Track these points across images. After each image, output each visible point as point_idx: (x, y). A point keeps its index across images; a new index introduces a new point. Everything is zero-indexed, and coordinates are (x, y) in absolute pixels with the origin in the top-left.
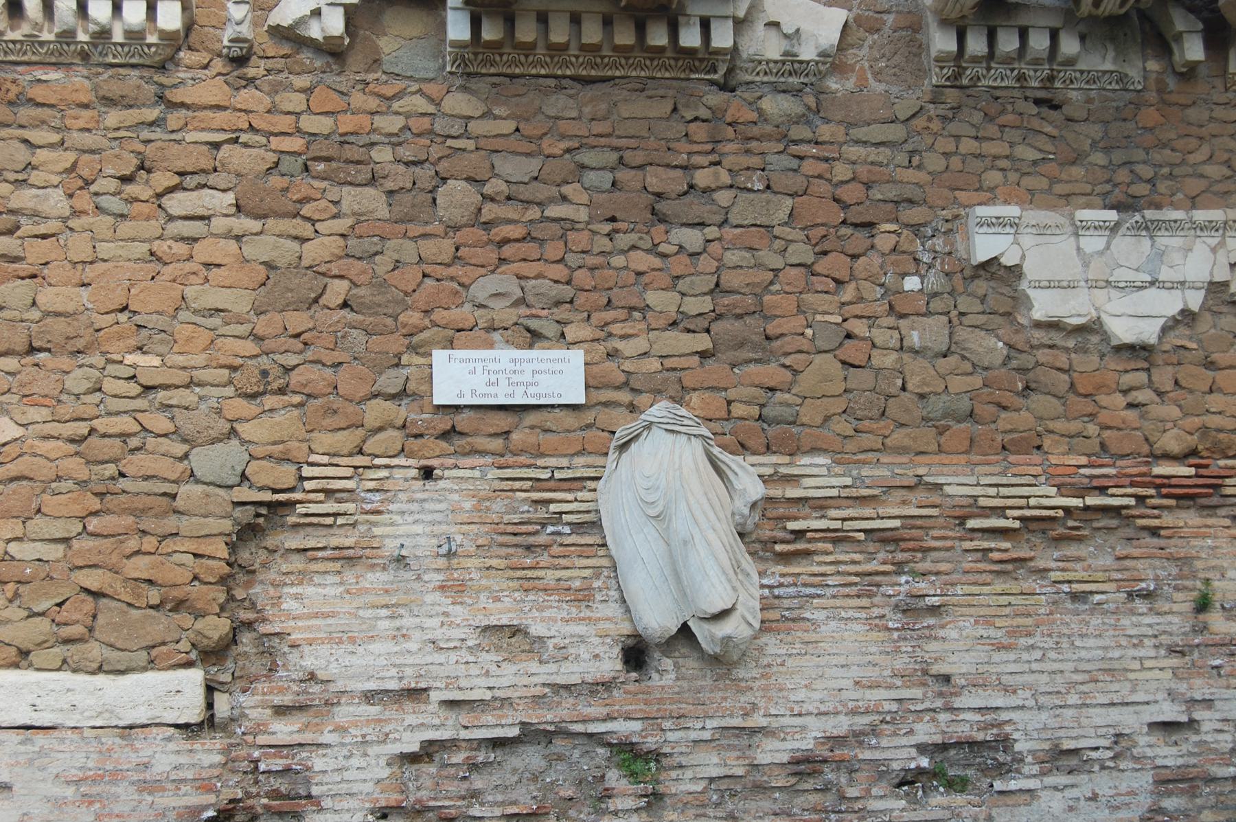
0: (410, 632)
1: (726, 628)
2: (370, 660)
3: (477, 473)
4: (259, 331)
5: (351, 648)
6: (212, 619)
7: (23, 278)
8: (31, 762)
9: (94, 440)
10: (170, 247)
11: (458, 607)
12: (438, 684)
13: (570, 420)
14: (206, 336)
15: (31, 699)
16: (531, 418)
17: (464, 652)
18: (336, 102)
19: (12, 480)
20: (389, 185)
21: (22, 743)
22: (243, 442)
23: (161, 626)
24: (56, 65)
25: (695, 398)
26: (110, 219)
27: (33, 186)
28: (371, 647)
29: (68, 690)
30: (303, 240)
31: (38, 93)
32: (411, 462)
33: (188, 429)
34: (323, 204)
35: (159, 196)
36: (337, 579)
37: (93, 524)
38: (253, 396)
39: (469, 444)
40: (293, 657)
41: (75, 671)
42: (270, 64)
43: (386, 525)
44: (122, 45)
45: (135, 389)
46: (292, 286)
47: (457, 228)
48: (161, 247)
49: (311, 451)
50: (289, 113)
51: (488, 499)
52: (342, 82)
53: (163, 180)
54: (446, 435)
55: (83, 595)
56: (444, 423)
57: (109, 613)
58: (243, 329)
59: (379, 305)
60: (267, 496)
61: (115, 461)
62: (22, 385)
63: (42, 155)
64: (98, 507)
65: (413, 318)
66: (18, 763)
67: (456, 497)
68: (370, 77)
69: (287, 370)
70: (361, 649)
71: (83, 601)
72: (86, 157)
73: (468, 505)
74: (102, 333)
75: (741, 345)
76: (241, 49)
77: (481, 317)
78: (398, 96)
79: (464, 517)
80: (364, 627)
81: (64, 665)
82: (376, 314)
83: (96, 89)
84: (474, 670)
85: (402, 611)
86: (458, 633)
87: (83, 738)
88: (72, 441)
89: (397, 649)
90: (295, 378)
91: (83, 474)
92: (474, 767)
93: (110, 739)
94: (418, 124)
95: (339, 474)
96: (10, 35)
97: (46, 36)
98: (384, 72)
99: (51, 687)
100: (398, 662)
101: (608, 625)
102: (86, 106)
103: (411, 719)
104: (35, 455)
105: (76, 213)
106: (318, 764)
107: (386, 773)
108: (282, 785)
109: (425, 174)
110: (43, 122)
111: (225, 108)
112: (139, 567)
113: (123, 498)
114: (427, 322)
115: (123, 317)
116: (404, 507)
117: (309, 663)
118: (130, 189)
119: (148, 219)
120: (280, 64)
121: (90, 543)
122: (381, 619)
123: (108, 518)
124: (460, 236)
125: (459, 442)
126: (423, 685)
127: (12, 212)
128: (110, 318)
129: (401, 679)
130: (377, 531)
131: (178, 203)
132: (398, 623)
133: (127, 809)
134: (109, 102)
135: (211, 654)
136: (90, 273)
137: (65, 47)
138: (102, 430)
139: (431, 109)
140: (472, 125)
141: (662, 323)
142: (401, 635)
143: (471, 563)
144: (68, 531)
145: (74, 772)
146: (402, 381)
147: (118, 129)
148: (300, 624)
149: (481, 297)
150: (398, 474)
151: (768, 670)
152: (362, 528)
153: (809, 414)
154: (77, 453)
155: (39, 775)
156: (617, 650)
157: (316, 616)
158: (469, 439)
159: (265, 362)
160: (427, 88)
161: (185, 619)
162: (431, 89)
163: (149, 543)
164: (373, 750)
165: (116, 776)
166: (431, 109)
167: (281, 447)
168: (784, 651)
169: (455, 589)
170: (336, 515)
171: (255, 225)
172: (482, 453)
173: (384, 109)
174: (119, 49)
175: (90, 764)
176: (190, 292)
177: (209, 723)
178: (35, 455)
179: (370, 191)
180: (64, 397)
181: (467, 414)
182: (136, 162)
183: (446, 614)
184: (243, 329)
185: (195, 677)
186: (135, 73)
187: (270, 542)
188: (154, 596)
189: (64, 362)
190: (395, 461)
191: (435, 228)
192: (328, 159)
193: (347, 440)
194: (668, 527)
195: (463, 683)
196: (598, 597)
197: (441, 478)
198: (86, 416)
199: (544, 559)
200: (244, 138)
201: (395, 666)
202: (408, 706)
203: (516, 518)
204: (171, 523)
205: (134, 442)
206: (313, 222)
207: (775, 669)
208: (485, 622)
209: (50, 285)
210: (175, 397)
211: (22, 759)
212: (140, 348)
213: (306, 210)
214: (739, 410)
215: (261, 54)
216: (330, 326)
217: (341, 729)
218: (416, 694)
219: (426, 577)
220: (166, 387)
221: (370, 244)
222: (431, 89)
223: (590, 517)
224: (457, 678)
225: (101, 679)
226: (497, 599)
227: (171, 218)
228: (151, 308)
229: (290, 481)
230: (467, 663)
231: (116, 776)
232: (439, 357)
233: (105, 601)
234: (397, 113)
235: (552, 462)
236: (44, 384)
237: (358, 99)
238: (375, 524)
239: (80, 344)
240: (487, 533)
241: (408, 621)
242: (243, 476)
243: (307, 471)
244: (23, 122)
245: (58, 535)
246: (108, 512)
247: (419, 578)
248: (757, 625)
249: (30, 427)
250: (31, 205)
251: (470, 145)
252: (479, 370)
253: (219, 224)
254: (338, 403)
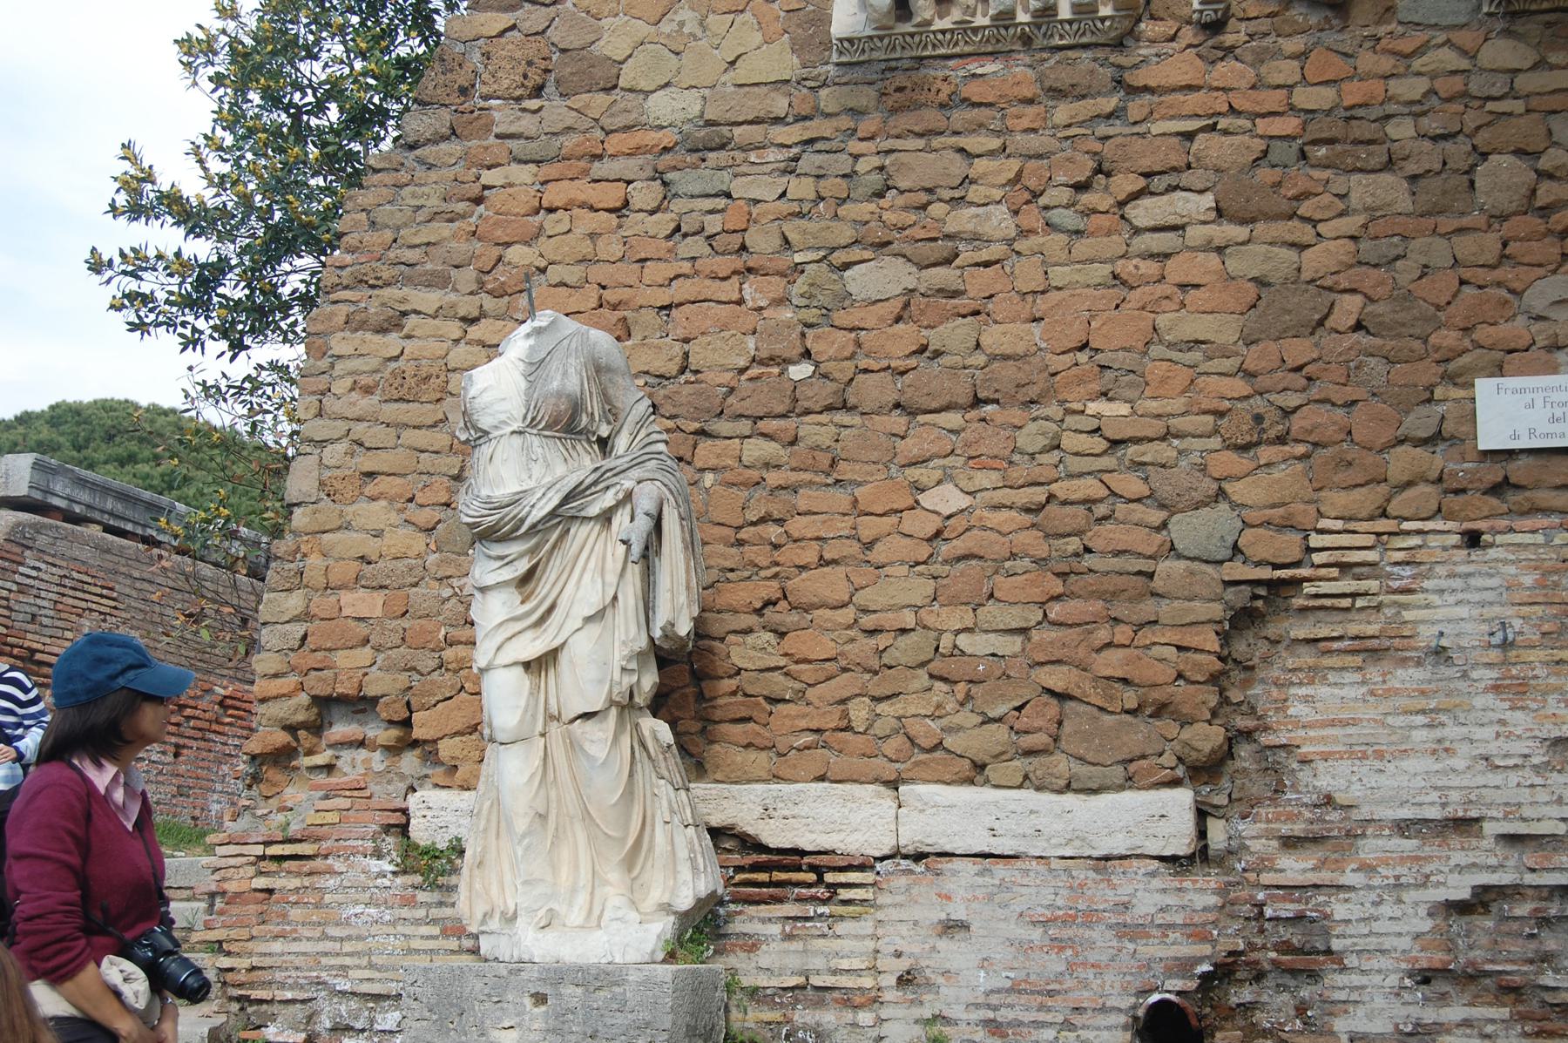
0: (1455, 745)
2: (1403, 781)
3: (1540, 538)
4: (1250, 365)
5: (1378, 764)
6: (1201, 727)
7: (964, 316)
8: (990, 897)
9: (1052, 508)
10: (1136, 267)
11: (1519, 714)
12: (1494, 813)
14: (1183, 375)
15: (989, 821)
17: (1527, 772)
18: (1339, 67)
19: (959, 559)
20: (1412, 168)
21: (980, 874)
22: (1234, 506)
23: (1139, 735)
24: (993, 54)
26: (1064, 238)
27: (971, 204)
28: (1404, 764)
29: (1032, 812)
30: (1302, 247)
31: (974, 91)
32: (1450, 525)
33: (1165, 491)
34: (1326, 199)
35: (1121, 204)
36: (1357, 677)
37: (1055, 611)
38: (1245, 448)
39: (1527, 499)
40: (1304, 775)
41: (1038, 789)
42: (1252, 26)
43: (1419, 607)
44: (1070, 22)
45: (1099, 444)
46: (1290, 307)
47: (1503, 218)
48: (1126, 268)
49: (1321, 515)
50: (1278, 87)
51: (1556, 571)
52: (1346, 41)
53: (1125, 183)
54: (1496, 489)
55: (1046, 698)
56: (1494, 474)
57: (1077, 718)
58: (1229, 364)
59: (1404, 325)
60: (1266, 573)
61: (1079, 533)
62: (968, 445)
63: (981, 165)
64: (1060, 590)
65: (1448, 338)
66: (975, 898)
67: (1512, 570)
68: (1382, 30)
69: (1287, 413)
70: (1391, 767)
71: (1046, 704)
72: (1033, 163)
73: (1528, 580)
74: (1058, 378)
76: (1216, 11)
77: (1540, 332)
78: (1419, 51)
79: (1525, 596)
80: (1394, 738)
81: (1025, 781)
82: (1399, 336)
83: (1040, 79)
84: (1543, 796)
85: (1443, 718)
86: (1520, 747)
87: (1051, 870)
88: (1028, 510)
89: (1438, 766)
90: (1297, 423)
91: (1042, 552)
92: (1544, 922)
93: (1082, 873)
94: (1446, 86)
95: (1358, 544)
96: (939, 24)
97: (981, 21)
98: (1400, 23)
99: (1012, 807)
100: (1440, 783)
102: (1030, 101)
103: (1459, 858)
104: (984, 528)
105: (1024, 233)
106: (1339, 911)
107: (1426, 925)
108: (1294, 936)
109: (1458, 151)
110: (981, 125)
111: (1198, 88)
112: (1111, 663)
113: (1090, 578)
114: (1467, 343)
115: (1082, 357)
116: (1444, 584)
117: (1324, 783)
118: (1086, 199)
119: (1109, 234)
120: (1264, 25)
121: (1053, 634)
122: (1416, 728)
123: (1072, 603)
124: (1507, 229)
125: (1514, 498)
126: (1474, 814)
127: (948, 237)
128: (1068, 358)
129: (1444, 805)
130: (1408, 615)
131: (1142, 213)
132: (1438, 733)
133: (1104, 958)
134: (1057, 93)
135: (1202, 771)
136: (1042, 304)
137: (1003, 32)
138: (1062, 495)
139: (1464, 64)
140: (1520, 81)
142: (1442, 749)
143: (1534, 656)
144: (1026, 620)
145: (1040, 910)
146: (1436, 421)
147: (1069, 126)
148: (1312, 733)
149: (1539, 306)
150: (1434, 541)
152: (1389, 612)
154: (1033, 525)
155: (1000, 913)
157: (1332, 723)
158: (1528, 494)
159: (1258, 404)
160: (1456, 37)
161: (1168, 726)
162: (1465, 38)
163: (1123, 634)
164: (1409, 896)
165: (1090, 917)
166: (1464, 64)
167: (1281, 510)
169: (1515, 690)
170: (1354, 595)
171: (1241, 232)
172: (1546, 511)
173: (1402, 70)
174: (1067, 27)
175: (1060, 902)
176: (1162, 321)
177: (1201, 856)
178: (984, 528)
179: (1386, 178)
180: (1016, 458)
181: (1523, 461)
182: (1091, 164)
183: (1502, 722)
184: (1229, 364)
185: (1181, 799)
186: (1086, 55)
187: (1271, 630)
188: (1130, 698)
189: (1016, 415)
190: (1430, 525)
191: (1475, 218)
192: (1330, 141)
193: (1365, 499)
195: (1527, 812)
197: (1492, 545)
198: (1042, 480)
200: (1223, 123)
201: (1435, 788)
202: (1455, 841)
204: (1148, 608)
205: (1101, 510)
206: (1314, 222)
208: (1556, 733)
209: (996, 322)
210: (1149, 453)
211: (979, 893)
212: (1105, 394)
213: (1305, 209)
215: (1241, 15)
216: (1340, 354)
217: (1367, 868)
218: (1464, 825)
219: (1475, 675)
220: (1137, 441)
221: (1389, 247)
222: (1465, 38)
224: (1519, 805)
225: (1069, 799)
227: (1137, 231)
228: (1116, 344)
229: (1295, 554)
230: (1532, 786)
231: (1090, 917)
232: (1485, 388)
233: (1072, 704)
234: (1419, 74)
236: (993, 443)
237: (1367, 61)
238: (1406, 606)
239: (1033, 392)
240: (1555, 616)
241: (1452, 731)
242: (1236, 549)
243: (1316, 541)
244: (958, 127)
245: (1014, 625)
246: (1072, 595)
247: (1465, 676)
249: (978, 495)
250: (970, 227)
251: (1518, 106)
252: (1539, 403)
253: (1196, 234)
254: (1353, 453)
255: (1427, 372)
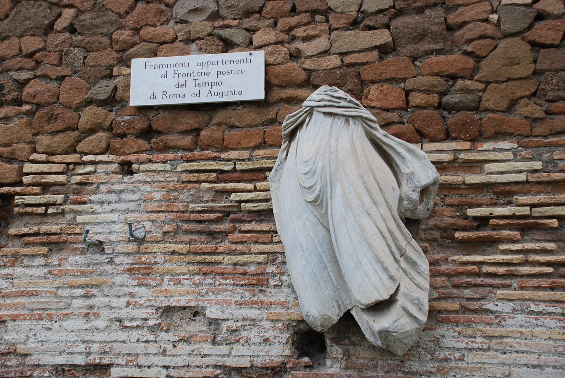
0: (100, 311)
1: (384, 322)
2: (63, 335)
3: (168, 167)
5: (48, 324)
11: (143, 289)
12: (119, 361)
13: (251, 116)
16: (219, 116)
17: (145, 332)
25: (373, 91)
28: (65, 324)
32: (112, 157)
36: (42, 261)
39: (161, 141)
43: (87, 213)
46: (29, 15)
49: (35, 151)
51: (176, 190)
56: (141, 124)
59: (97, 27)
65: (124, 35)
67: (147, 188)
69: (22, 84)
70: (56, 325)
73: (158, 195)
75: (421, 37)
77: (180, 30)
79: (153, 206)
80: (61, 305)
82: (94, 34)
84: (152, 348)
85: (95, 291)
86: (141, 313)
89: (87, 326)
90: (27, 90)
100: (86, 338)
101: (280, 310)
114: (136, 39)
116: (103, 197)
122: (76, 298)
126: (106, 361)
129: (88, 354)
130: (80, 219)
132: (90, 302)
141: (342, 22)
142: (89, 314)
143: (156, 248)
146: (110, 89)
148: (8, 301)
150: (101, 168)
151: (444, 364)
152: (69, 217)
153: (490, 99)
156: (286, 335)
157: (22, 294)
158: (163, 137)
167: (9, 149)
168: (463, 345)
169: (141, 271)
170: (47, 205)
172: (175, 148)
183: (132, 295)
190: (99, 158)
194: (326, 212)
195: (142, 361)
196: (272, 282)
197: (138, 171)
199: (224, 246)
201: (84, 342)
203: (198, 207)
207: (453, 364)
208: (166, 303)
214: (416, 99)
216: (57, 46)
219: (117, 260)
223: (263, 206)
224: (137, 355)
226: (178, 282)
229: (12, 177)
230: (147, 341)
235: (234, 154)
238: (80, 213)
240: (173, 220)
247: (111, 262)
248: (423, 318)
252: (171, 74)
255: (108, 57)
